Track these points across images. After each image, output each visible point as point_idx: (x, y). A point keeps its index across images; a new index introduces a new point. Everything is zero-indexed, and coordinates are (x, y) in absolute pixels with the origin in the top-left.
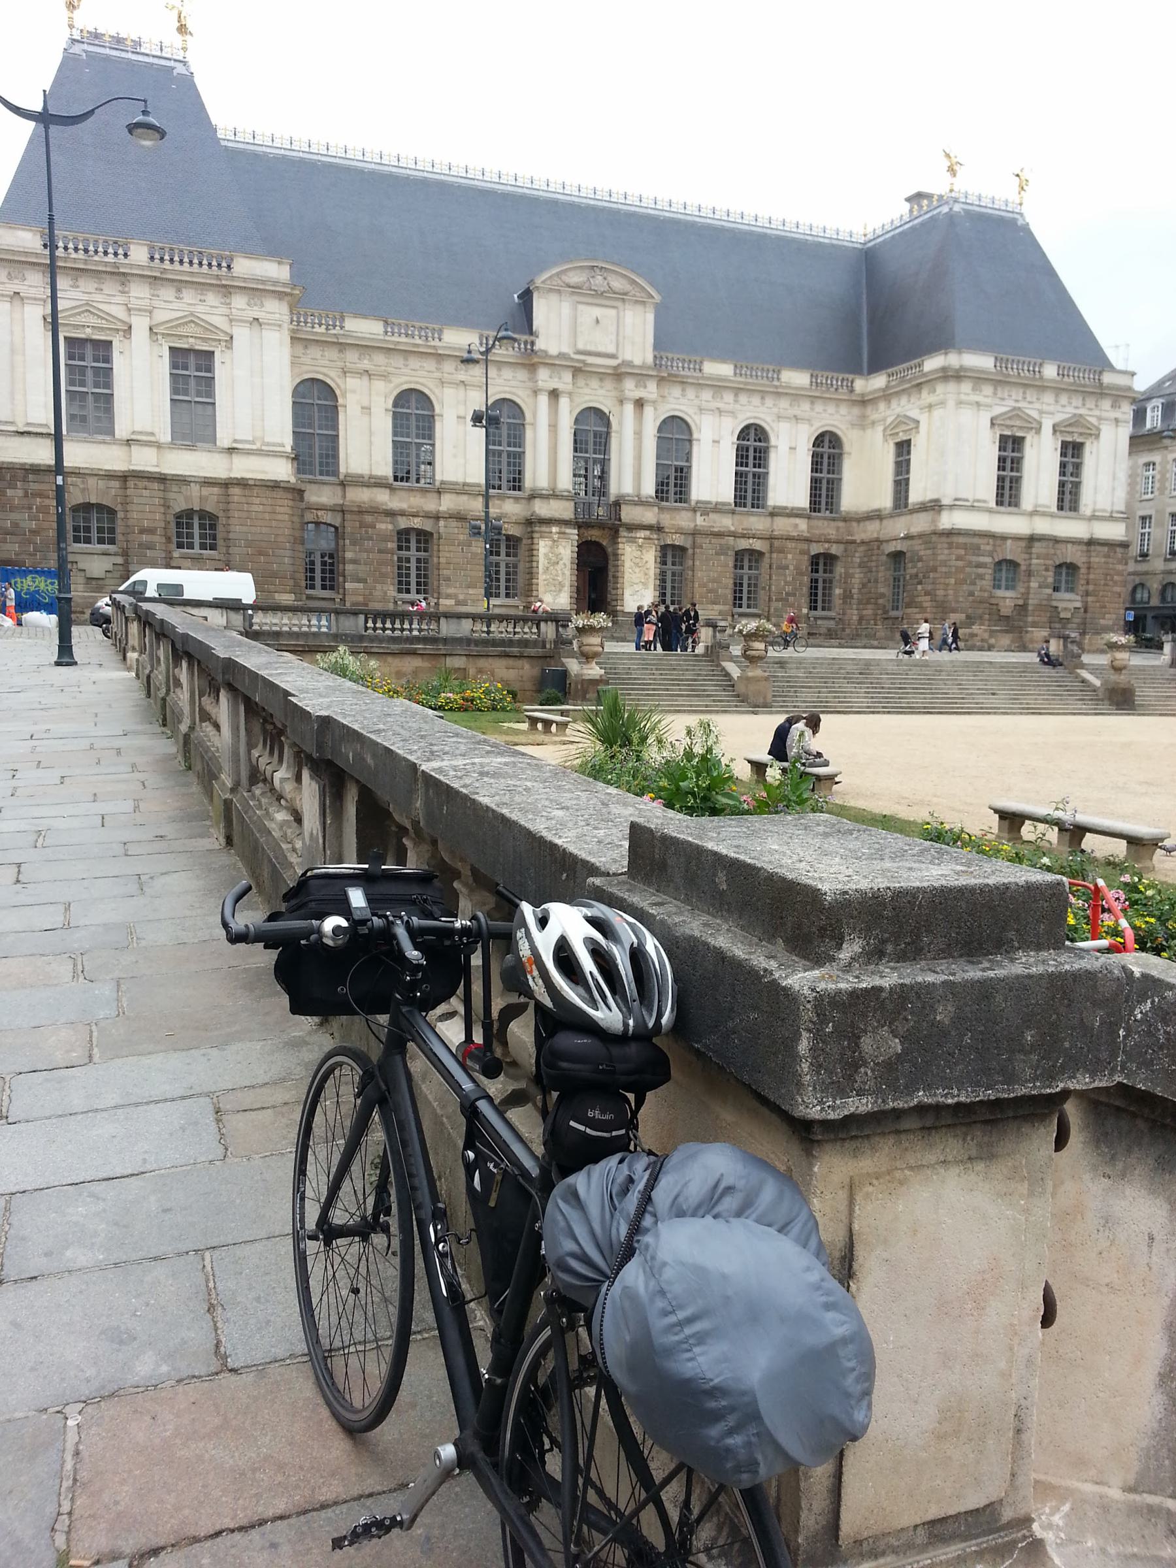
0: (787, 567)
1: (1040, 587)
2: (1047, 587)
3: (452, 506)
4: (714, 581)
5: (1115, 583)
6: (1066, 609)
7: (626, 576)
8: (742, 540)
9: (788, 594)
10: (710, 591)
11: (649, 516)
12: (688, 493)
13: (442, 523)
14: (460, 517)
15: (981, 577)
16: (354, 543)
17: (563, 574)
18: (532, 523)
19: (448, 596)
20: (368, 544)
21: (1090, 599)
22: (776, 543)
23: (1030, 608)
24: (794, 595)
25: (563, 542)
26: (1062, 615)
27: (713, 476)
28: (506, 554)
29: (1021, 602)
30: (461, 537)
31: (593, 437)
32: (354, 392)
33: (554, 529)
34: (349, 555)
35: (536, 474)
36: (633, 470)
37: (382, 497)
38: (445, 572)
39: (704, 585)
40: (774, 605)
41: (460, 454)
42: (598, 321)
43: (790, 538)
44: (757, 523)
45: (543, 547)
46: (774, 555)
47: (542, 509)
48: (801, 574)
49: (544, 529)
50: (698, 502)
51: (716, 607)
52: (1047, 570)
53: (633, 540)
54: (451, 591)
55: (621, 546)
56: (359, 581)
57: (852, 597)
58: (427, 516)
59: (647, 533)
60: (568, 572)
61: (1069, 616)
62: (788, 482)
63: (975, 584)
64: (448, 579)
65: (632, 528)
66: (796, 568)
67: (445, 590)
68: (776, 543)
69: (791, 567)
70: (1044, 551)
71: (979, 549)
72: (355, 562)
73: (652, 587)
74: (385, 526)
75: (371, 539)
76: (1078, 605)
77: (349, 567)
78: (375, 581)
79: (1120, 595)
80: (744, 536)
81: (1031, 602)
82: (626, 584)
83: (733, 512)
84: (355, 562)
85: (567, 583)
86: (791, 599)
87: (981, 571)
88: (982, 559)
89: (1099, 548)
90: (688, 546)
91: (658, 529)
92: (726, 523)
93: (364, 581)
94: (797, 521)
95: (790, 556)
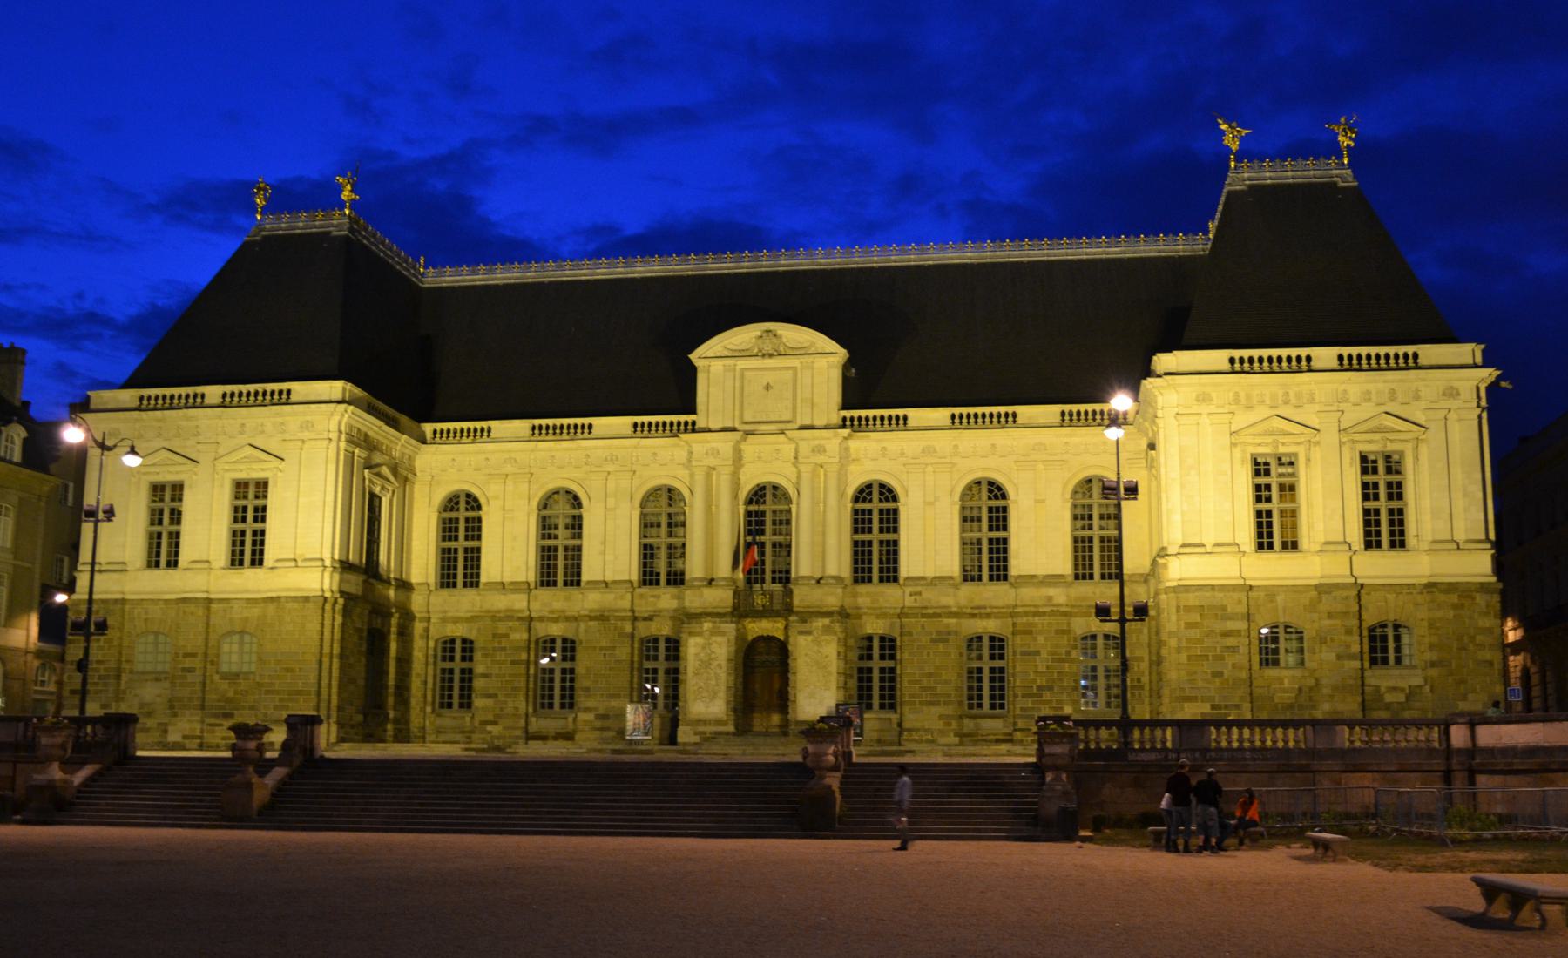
0: (1038, 653)
1: (1339, 657)
2: (1351, 657)
3: (595, 606)
4: (930, 675)
5: (1481, 646)
6: (1394, 689)
7: (799, 676)
8: (972, 621)
9: (1039, 688)
10: (924, 689)
11: (832, 599)
12: (896, 570)
13: (582, 626)
14: (601, 617)
15: (1234, 650)
16: (486, 656)
17: (717, 677)
18: (686, 618)
19: (587, 710)
20: (500, 656)
21: (1433, 672)
22: (1019, 620)
23: (1325, 691)
24: (1050, 688)
25: (719, 639)
26: (1389, 698)
27: (930, 543)
28: (660, 660)
29: (1311, 682)
30: (604, 644)
31: (764, 515)
32: (496, 498)
33: (707, 625)
34: (479, 669)
35: (694, 567)
36: (821, 546)
37: (519, 602)
38: (586, 683)
39: (916, 682)
40: (1020, 703)
41: (610, 549)
42: (768, 387)
43: (1044, 614)
44: (991, 593)
45: (692, 648)
46: (1018, 639)
47: (694, 599)
48: (1062, 660)
49: (694, 627)
50: (907, 578)
51: (933, 709)
52: (1349, 632)
53: (809, 633)
54: (590, 703)
55: (791, 640)
56: (489, 696)
57: (1142, 687)
58: (568, 619)
59: (827, 621)
60: (723, 675)
61: (1401, 698)
62: (1041, 542)
63: (1222, 658)
64: (587, 689)
65: (807, 616)
66: (1052, 653)
67: (581, 700)
68: (1019, 620)
69: (1044, 654)
70: (1340, 607)
71: (1224, 608)
72: (485, 676)
73: (834, 688)
74: (520, 636)
75: (504, 649)
76: (1417, 681)
77: (478, 684)
78: (507, 696)
79: (1491, 663)
80: (973, 616)
81: (1324, 681)
82: (800, 685)
83: (956, 587)
84: (485, 676)
85: (723, 688)
86: (1047, 695)
87: (1230, 641)
88: (1230, 625)
89: (1442, 597)
90: (896, 634)
91: (843, 614)
92: (948, 599)
93: (494, 696)
94: (1051, 591)
95: (1041, 639)
